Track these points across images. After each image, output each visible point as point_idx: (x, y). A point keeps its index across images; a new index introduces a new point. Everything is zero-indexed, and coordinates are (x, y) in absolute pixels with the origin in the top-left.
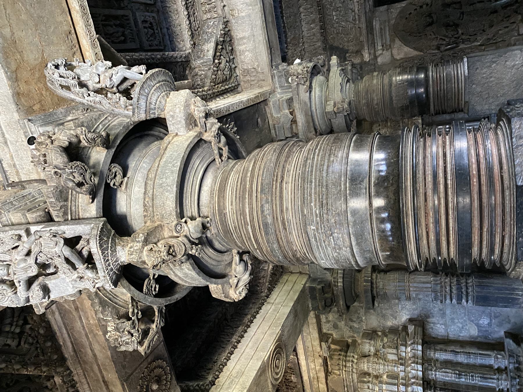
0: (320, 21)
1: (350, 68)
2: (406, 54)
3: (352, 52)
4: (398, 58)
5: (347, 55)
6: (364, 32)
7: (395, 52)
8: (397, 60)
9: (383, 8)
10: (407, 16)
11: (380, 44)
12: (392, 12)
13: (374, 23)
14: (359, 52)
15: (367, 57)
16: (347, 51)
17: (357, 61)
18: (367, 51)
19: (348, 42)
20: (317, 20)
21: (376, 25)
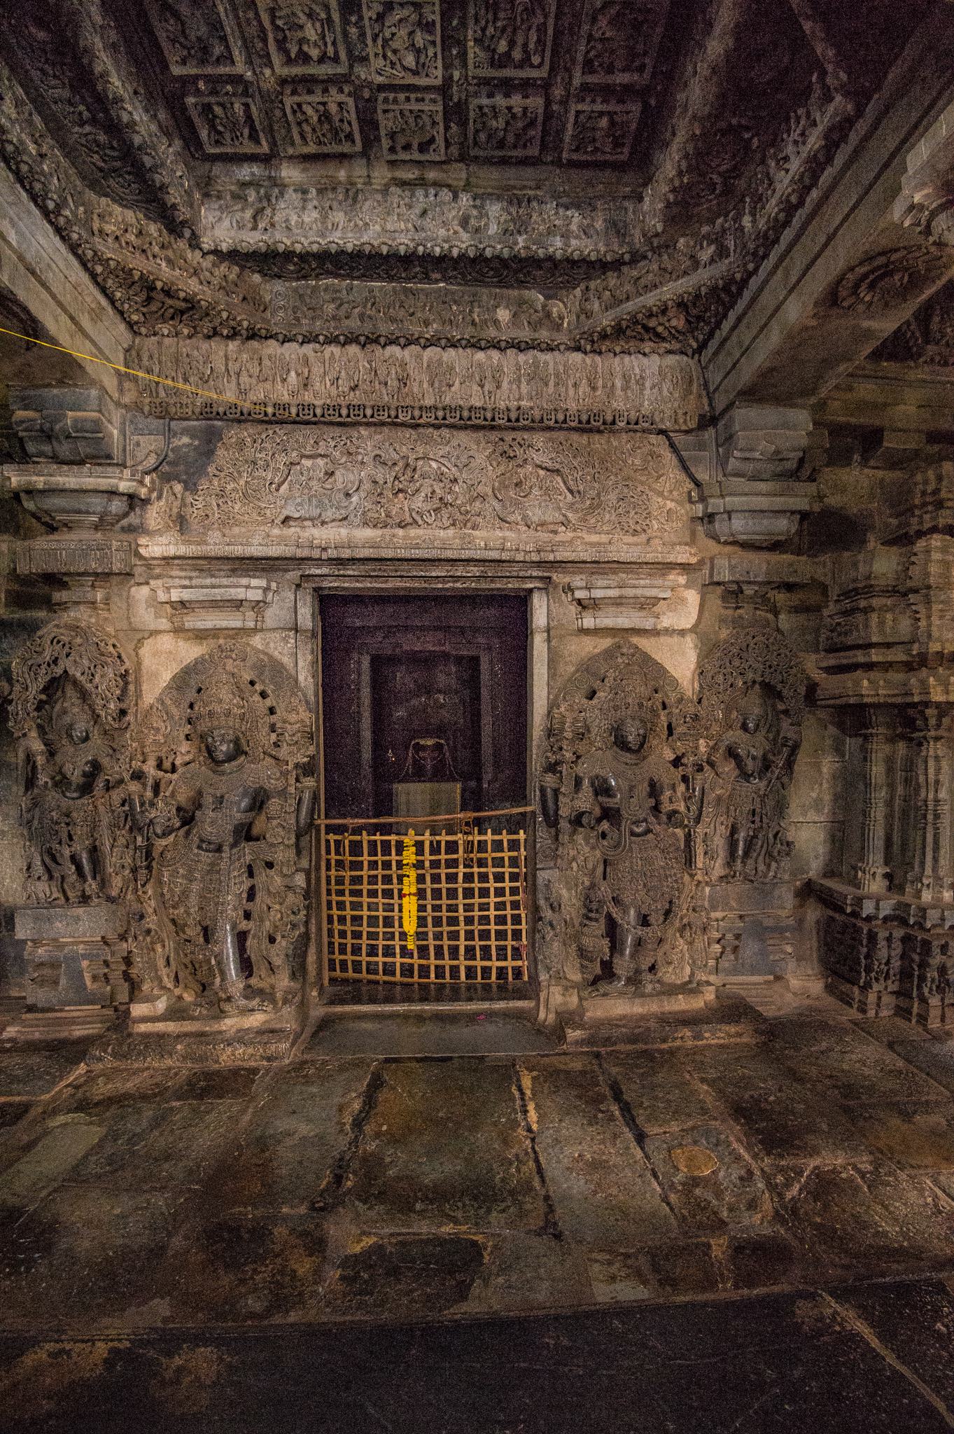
0: (302, 406)
1: (124, 486)
2: (156, 675)
3: (183, 504)
4: (145, 651)
5: (178, 488)
6: (238, 551)
7: (166, 642)
8: (136, 649)
9: (306, 615)
10: (258, 687)
11: (186, 595)
12: (285, 640)
13: (254, 582)
14: (181, 523)
15: (156, 547)
16: (190, 487)
17: (154, 516)
18: (172, 551)
19: (222, 494)
20: (308, 397)
21: (251, 588)
